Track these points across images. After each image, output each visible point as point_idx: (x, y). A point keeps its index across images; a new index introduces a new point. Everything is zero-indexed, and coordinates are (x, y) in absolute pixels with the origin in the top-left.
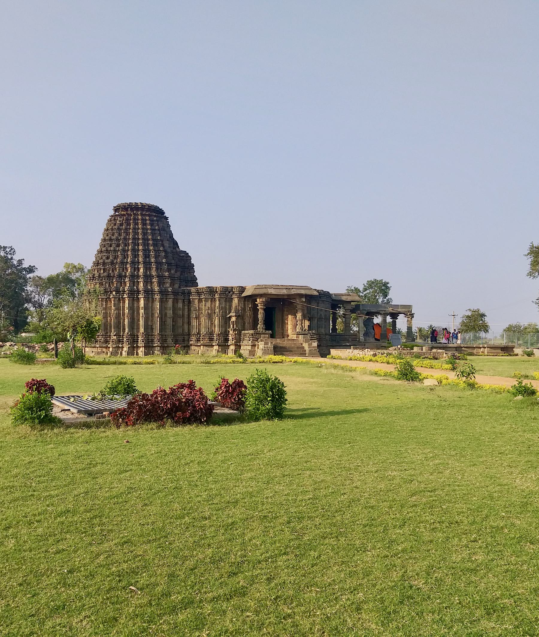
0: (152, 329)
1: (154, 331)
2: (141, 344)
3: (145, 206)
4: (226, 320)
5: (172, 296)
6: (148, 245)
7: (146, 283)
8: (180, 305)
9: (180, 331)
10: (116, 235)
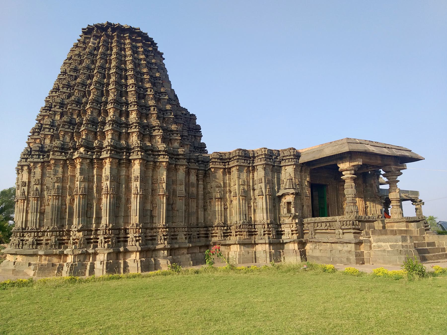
0: (152, 217)
1: (156, 220)
2: (133, 244)
4: (275, 200)
5: (184, 162)
6: (142, 80)
7: (142, 136)
9: (193, 220)
10: (87, 62)
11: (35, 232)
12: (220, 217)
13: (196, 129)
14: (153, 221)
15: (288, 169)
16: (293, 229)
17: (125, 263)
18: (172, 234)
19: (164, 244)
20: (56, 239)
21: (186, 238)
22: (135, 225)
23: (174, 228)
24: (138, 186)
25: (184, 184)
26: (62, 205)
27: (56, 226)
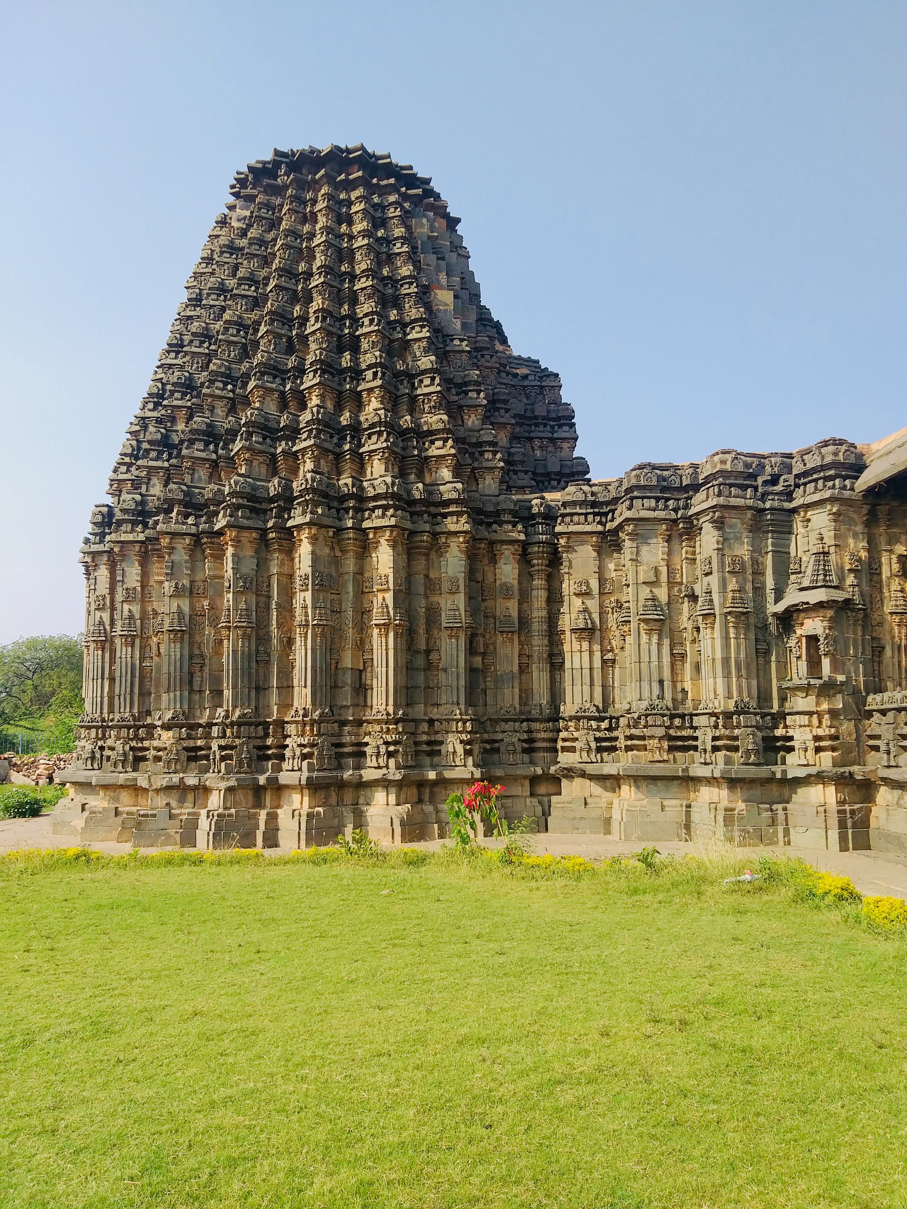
0: (362, 690)
3: (349, 151)
5: (461, 524)
8: (508, 571)
9: (510, 698)
11: (97, 728)
12: (586, 688)
13: (558, 419)
14: (365, 701)
15: (814, 519)
16: (820, 732)
17: (272, 817)
18: (425, 738)
19: (387, 767)
20: (127, 748)
21: (468, 753)
22: (301, 712)
23: (431, 722)
24: (309, 602)
25: (462, 588)
26: (142, 658)
27: (127, 715)
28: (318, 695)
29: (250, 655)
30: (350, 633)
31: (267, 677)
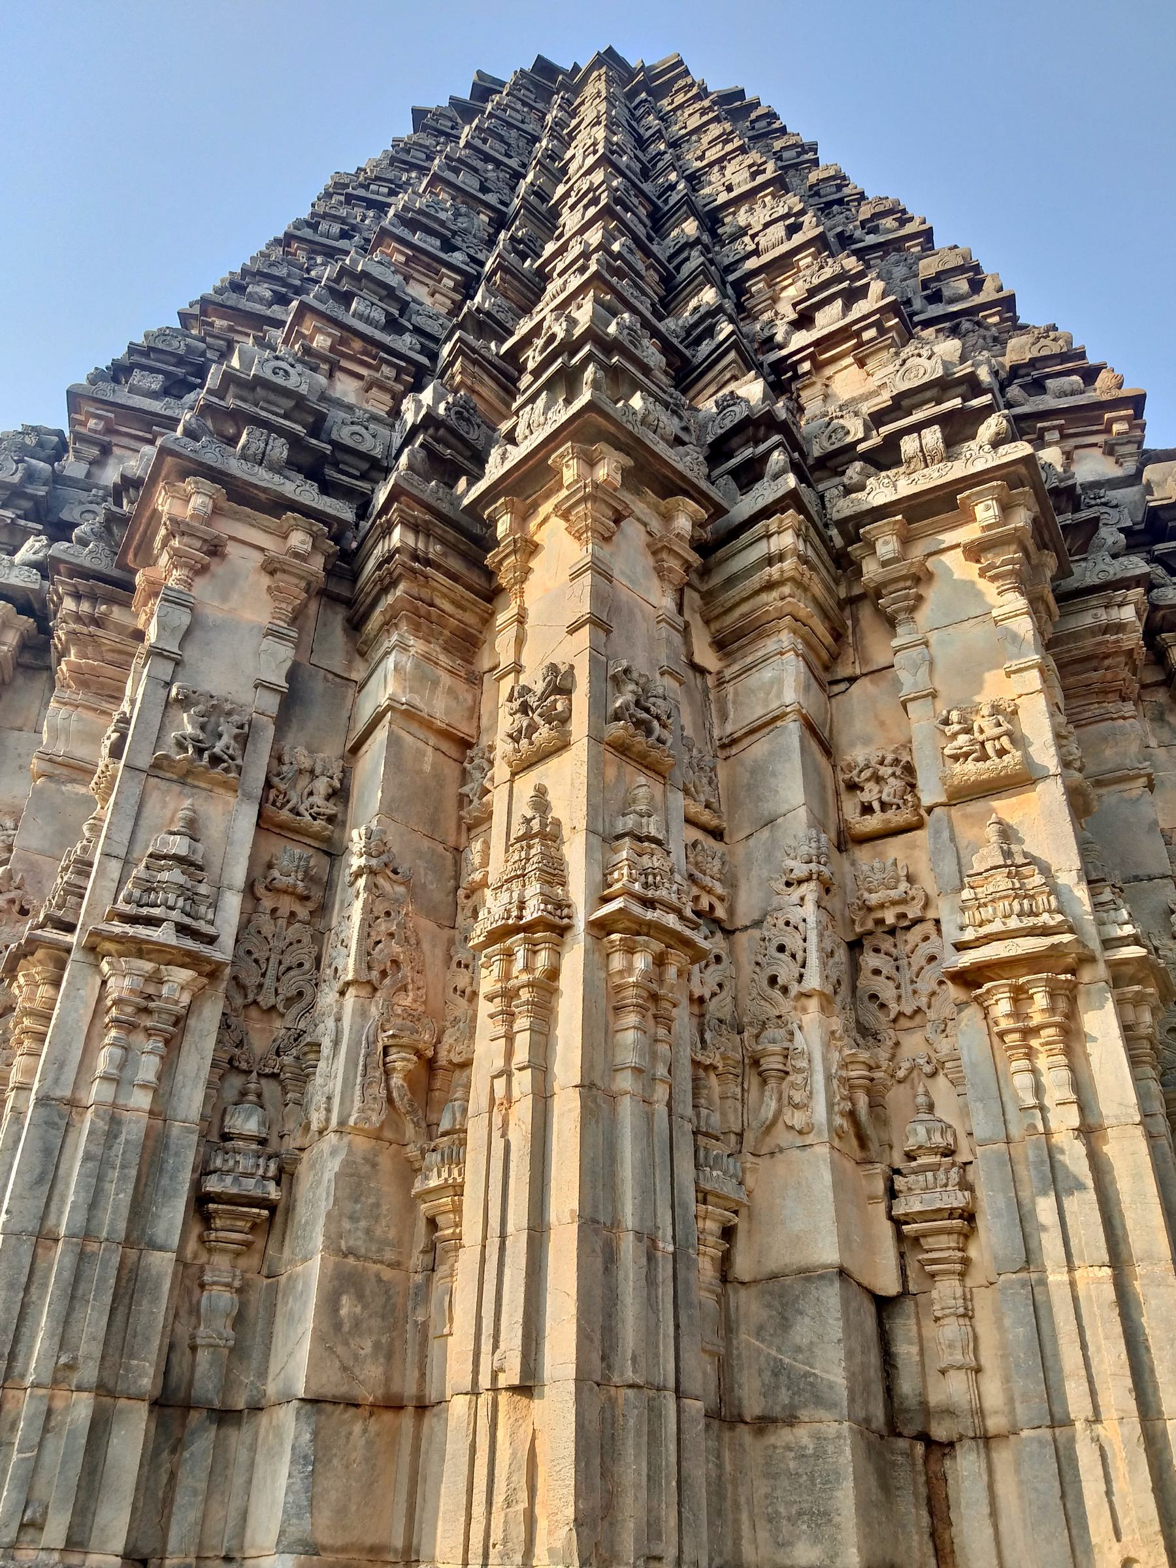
28: (632, 1469)
29: (155, 1147)
30: (812, 1030)
31: (250, 1330)
